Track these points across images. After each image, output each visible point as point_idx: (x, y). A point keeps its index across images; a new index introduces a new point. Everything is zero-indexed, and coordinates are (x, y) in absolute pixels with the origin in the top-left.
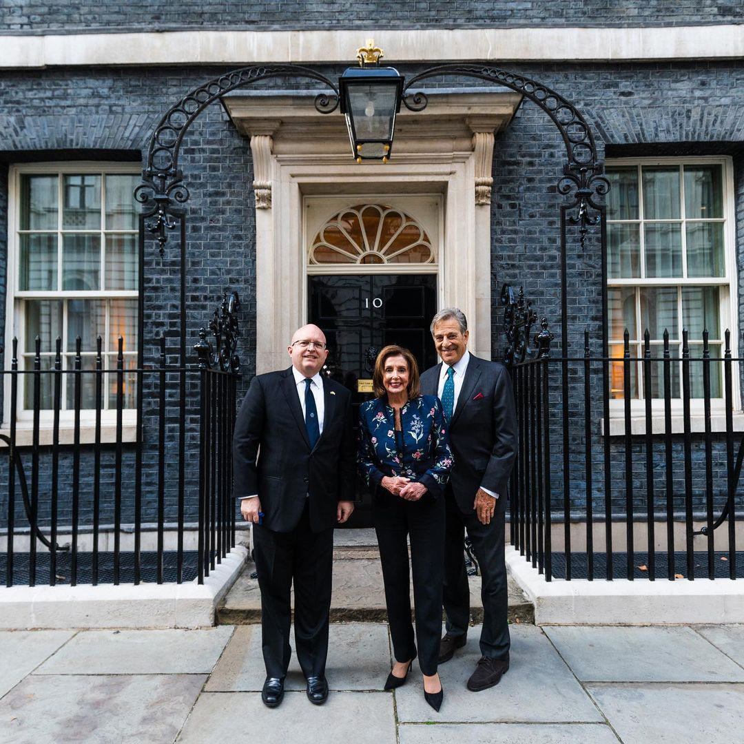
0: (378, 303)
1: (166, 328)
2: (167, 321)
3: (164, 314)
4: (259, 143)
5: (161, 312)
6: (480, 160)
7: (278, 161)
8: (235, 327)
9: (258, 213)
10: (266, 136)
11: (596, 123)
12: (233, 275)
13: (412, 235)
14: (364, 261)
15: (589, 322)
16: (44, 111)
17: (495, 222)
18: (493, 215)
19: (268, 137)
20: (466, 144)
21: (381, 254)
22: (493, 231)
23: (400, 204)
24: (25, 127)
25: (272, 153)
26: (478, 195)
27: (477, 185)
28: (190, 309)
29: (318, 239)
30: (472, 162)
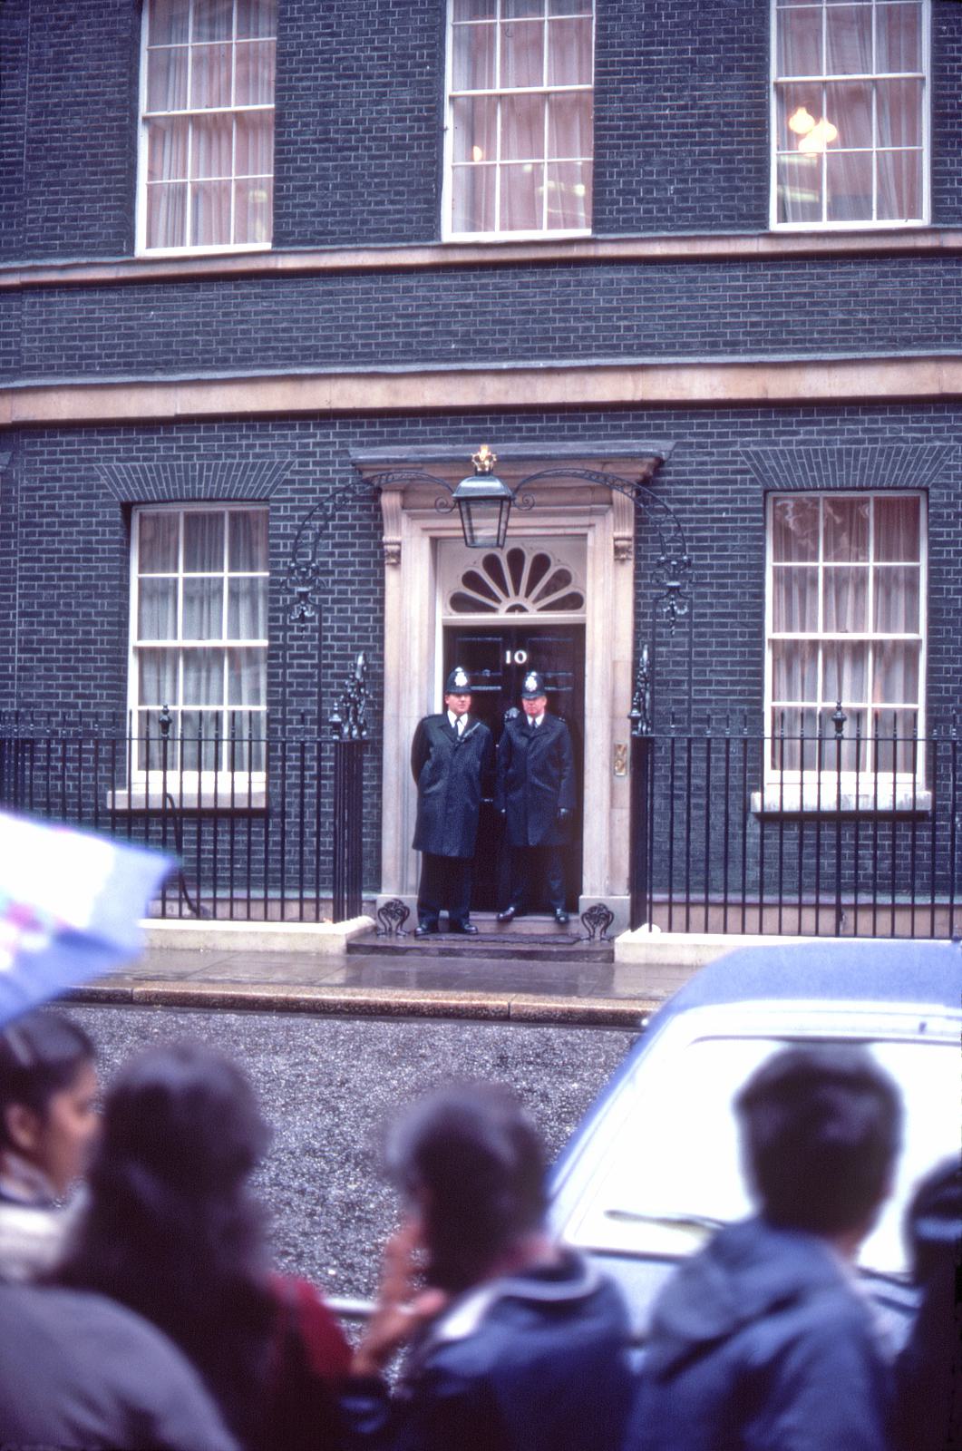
0: (521, 657)
4: (389, 501)
6: (620, 512)
7: (409, 515)
9: (388, 569)
11: (753, 465)
13: (563, 578)
14: (512, 609)
17: (638, 575)
18: (637, 567)
20: (605, 495)
22: (637, 586)
23: (545, 548)
25: (403, 508)
26: (617, 550)
27: (616, 539)
30: (611, 516)
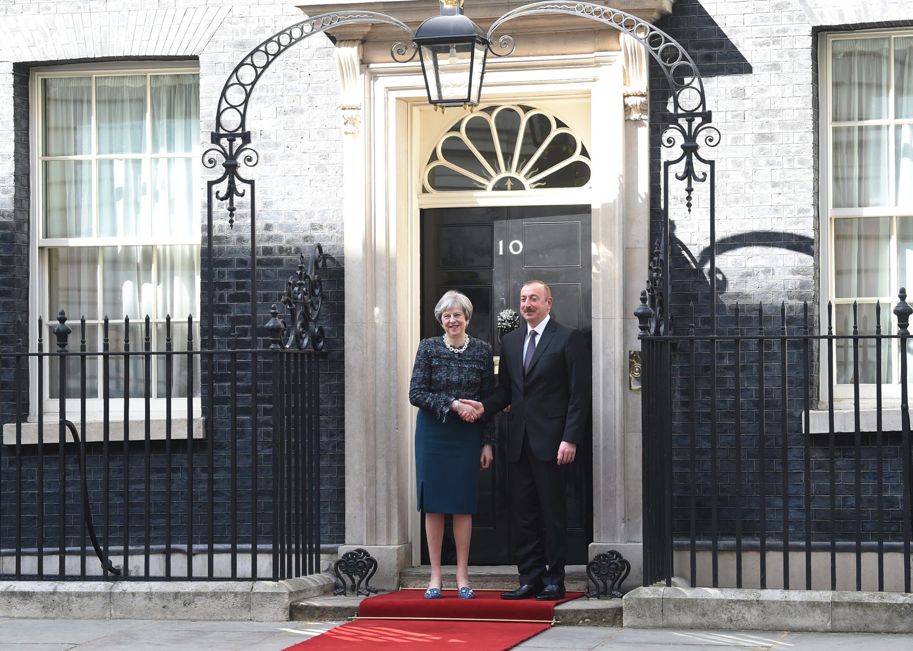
0: (516, 247)
1: (232, 291)
2: (233, 280)
3: (230, 272)
5: (226, 269)
8: (317, 291)
10: (354, 40)
12: (316, 219)
13: (565, 145)
14: (500, 186)
15: (790, 276)
16: (79, 8)
19: (357, 43)
21: (521, 177)
24: (55, 29)
28: (262, 265)
29: (434, 157)
